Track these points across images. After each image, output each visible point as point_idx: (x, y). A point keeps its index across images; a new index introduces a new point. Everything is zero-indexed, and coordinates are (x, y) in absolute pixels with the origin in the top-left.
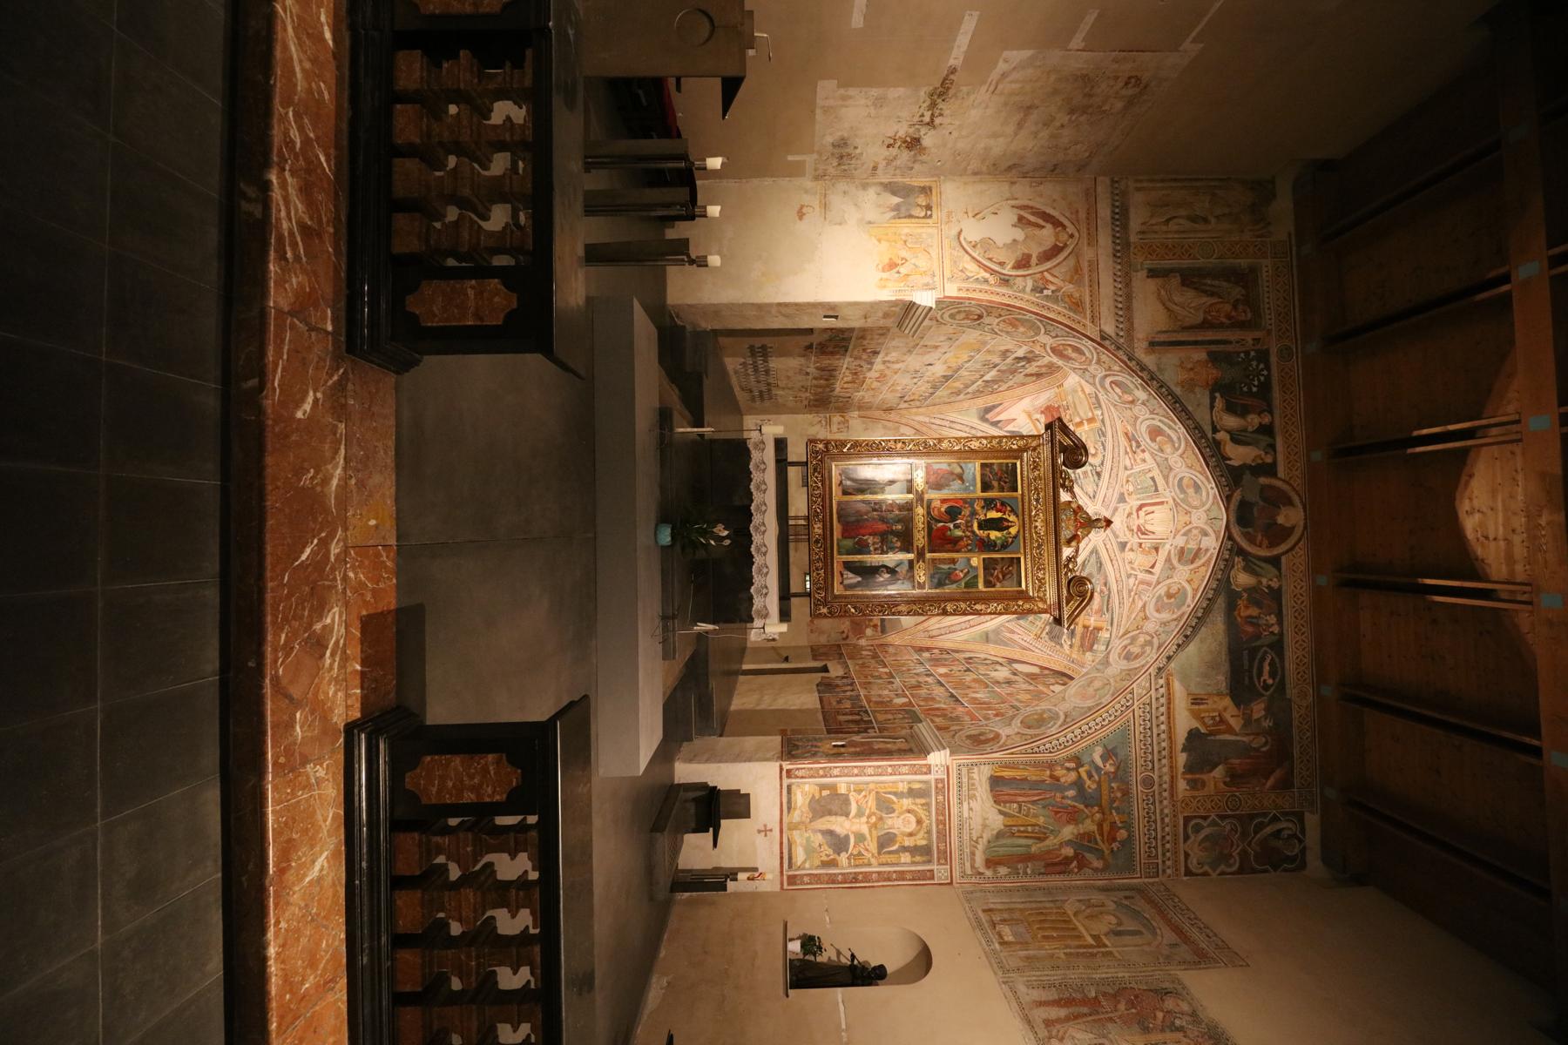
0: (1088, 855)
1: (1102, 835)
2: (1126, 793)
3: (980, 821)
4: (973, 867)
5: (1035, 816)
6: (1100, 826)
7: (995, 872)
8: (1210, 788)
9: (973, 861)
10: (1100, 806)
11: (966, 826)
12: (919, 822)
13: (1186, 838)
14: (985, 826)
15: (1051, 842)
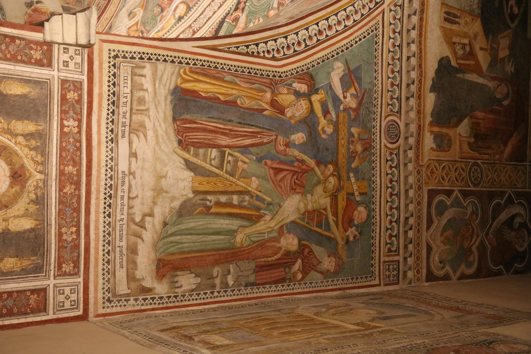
0: (317, 250)
1: (335, 214)
2: (368, 147)
3: (149, 179)
4: (131, 278)
5: (245, 176)
6: (334, 197)
7: (173, 284)
8: (455, 152)
9: (132, 264)
10: (336, 164)
11: (122, 191)
12: (18, 176)
13: (430, 222)
14: (159, 191)
15: (267, 225)
